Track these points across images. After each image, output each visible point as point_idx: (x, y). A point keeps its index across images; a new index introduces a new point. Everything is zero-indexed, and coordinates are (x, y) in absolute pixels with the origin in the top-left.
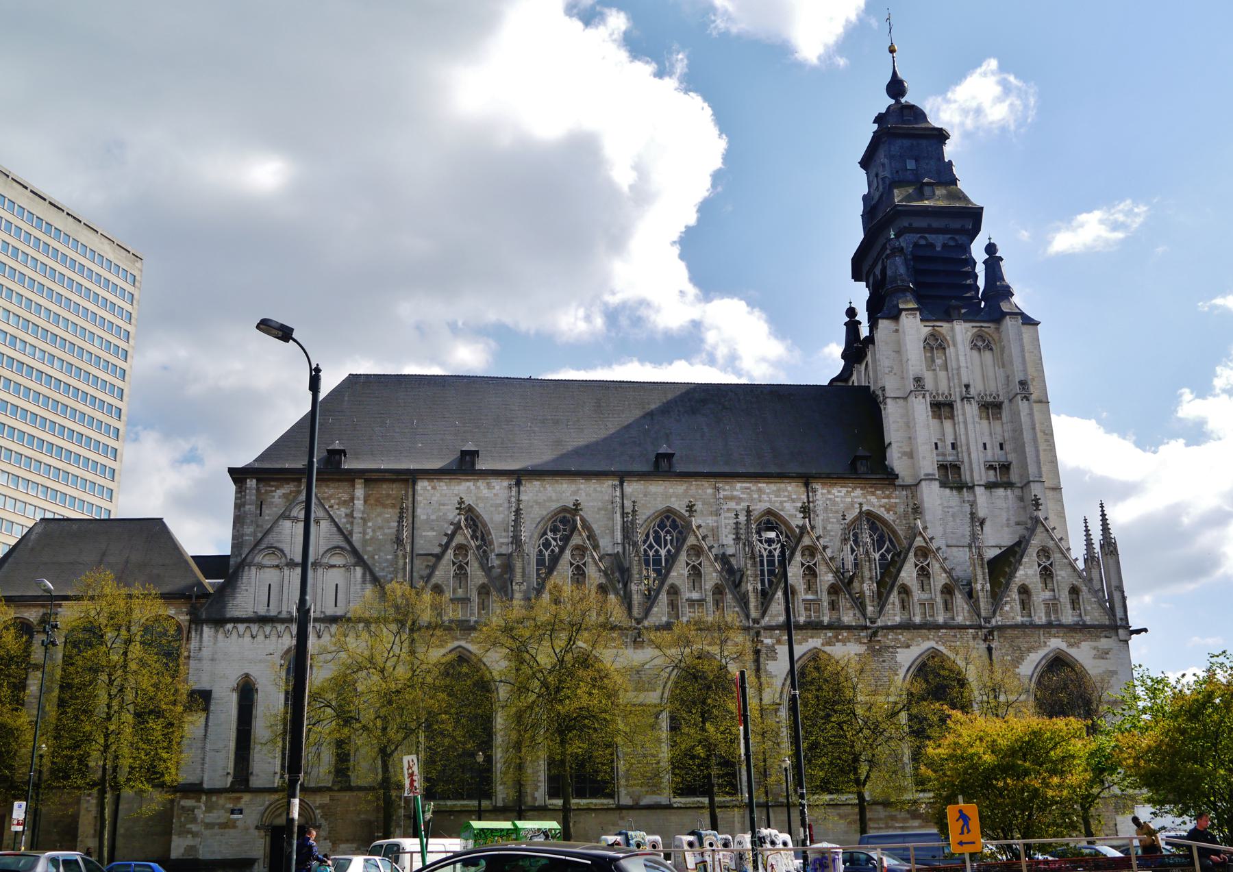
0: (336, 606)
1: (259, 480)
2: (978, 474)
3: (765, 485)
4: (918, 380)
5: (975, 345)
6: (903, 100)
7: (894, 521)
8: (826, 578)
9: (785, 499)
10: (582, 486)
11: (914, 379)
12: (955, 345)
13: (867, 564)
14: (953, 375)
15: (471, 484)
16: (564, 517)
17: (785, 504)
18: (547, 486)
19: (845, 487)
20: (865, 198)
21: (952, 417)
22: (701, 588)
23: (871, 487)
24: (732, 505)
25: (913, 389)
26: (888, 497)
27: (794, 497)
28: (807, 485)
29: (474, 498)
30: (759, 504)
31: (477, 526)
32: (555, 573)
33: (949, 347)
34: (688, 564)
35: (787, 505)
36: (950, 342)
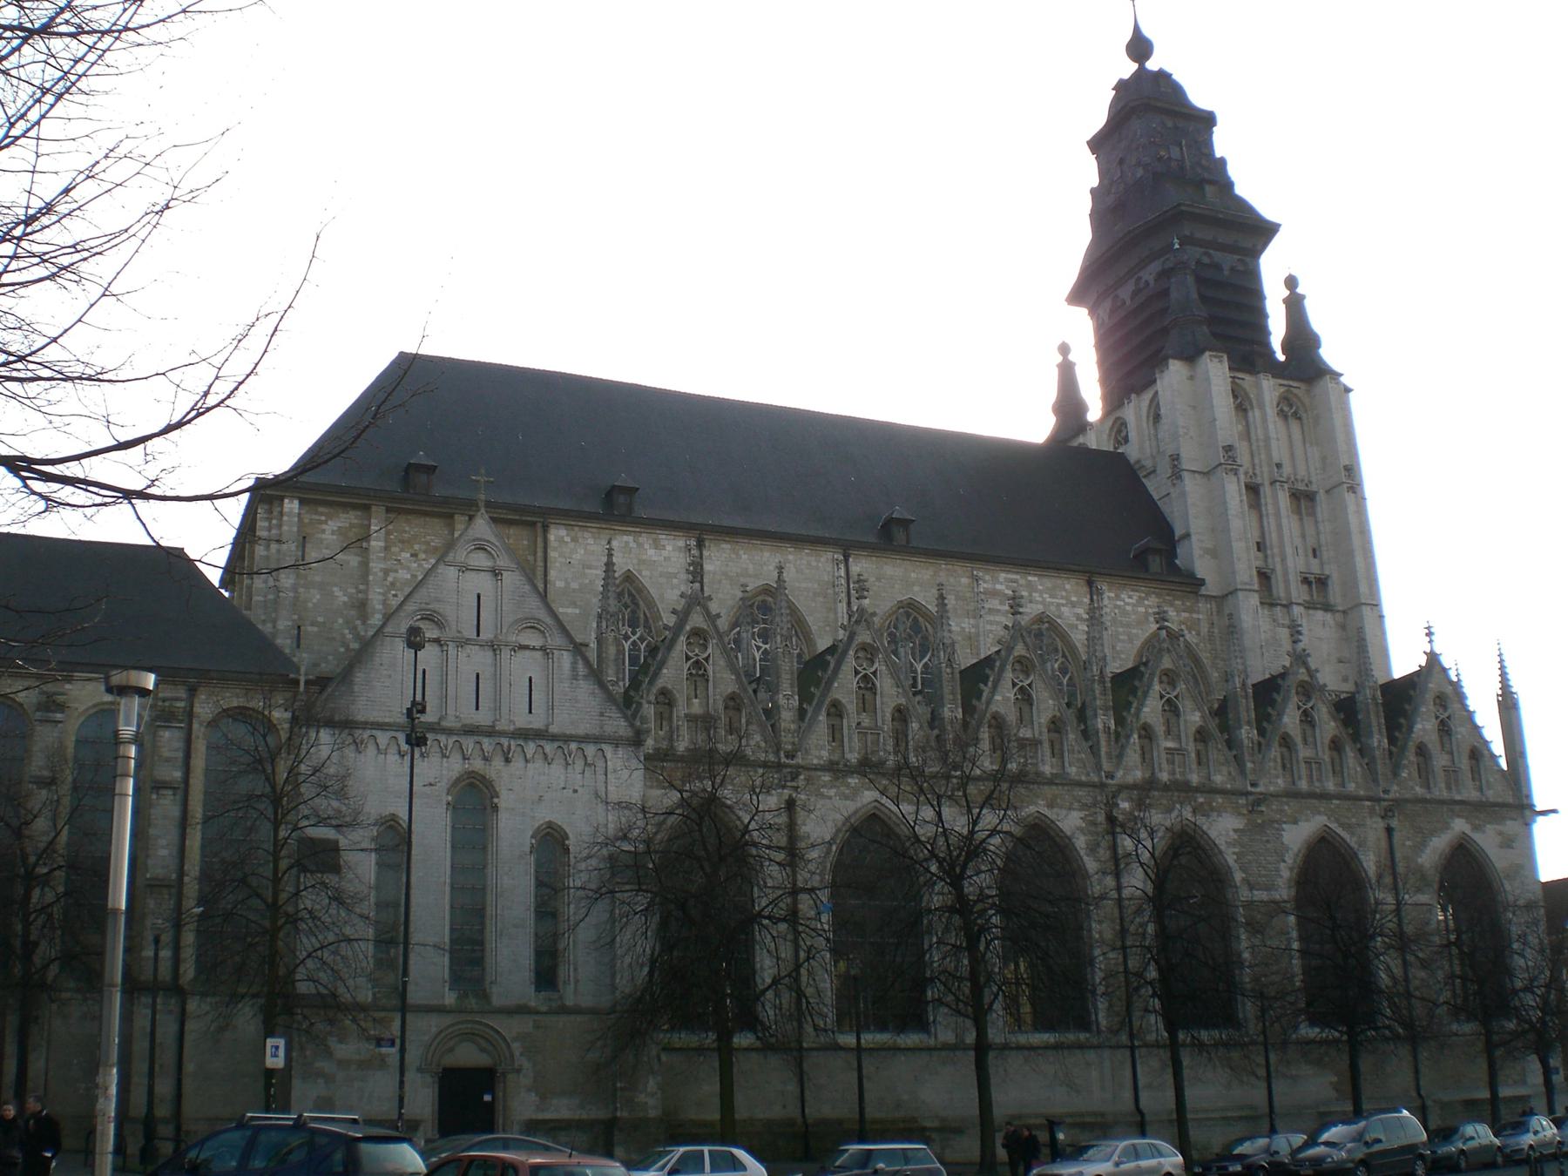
0: (530, 712)
1: (302, 502)
3: (1036, 579)
4: (1229, 449)
5: (1282, 410)
6: (1152, 65)
7: (1197, 645)
8: (1193, 718)
9: (1064, 602)
10: (791, 557)
11: (1223, 447)
12: (1262, 407)
13: (1244, 701)
14: (1258, 446)
15: (630, 538)
16: (764, 601)
17: (1062, 609)
18: (741, 552)
19: (1137, 591)
20: (1093, 191)
22: (1032, 723)
23: (1168, 595)
25: (1223, 461)
26: (1190, 610)
27: (1074, 599)
28: (1090, 583)
29: (635, 561)
30: (1029, 605)
31: (637, 605)
32: (836, 685)
33: (1252, 408)
34: (1014, 685)
36: (1254, 402)
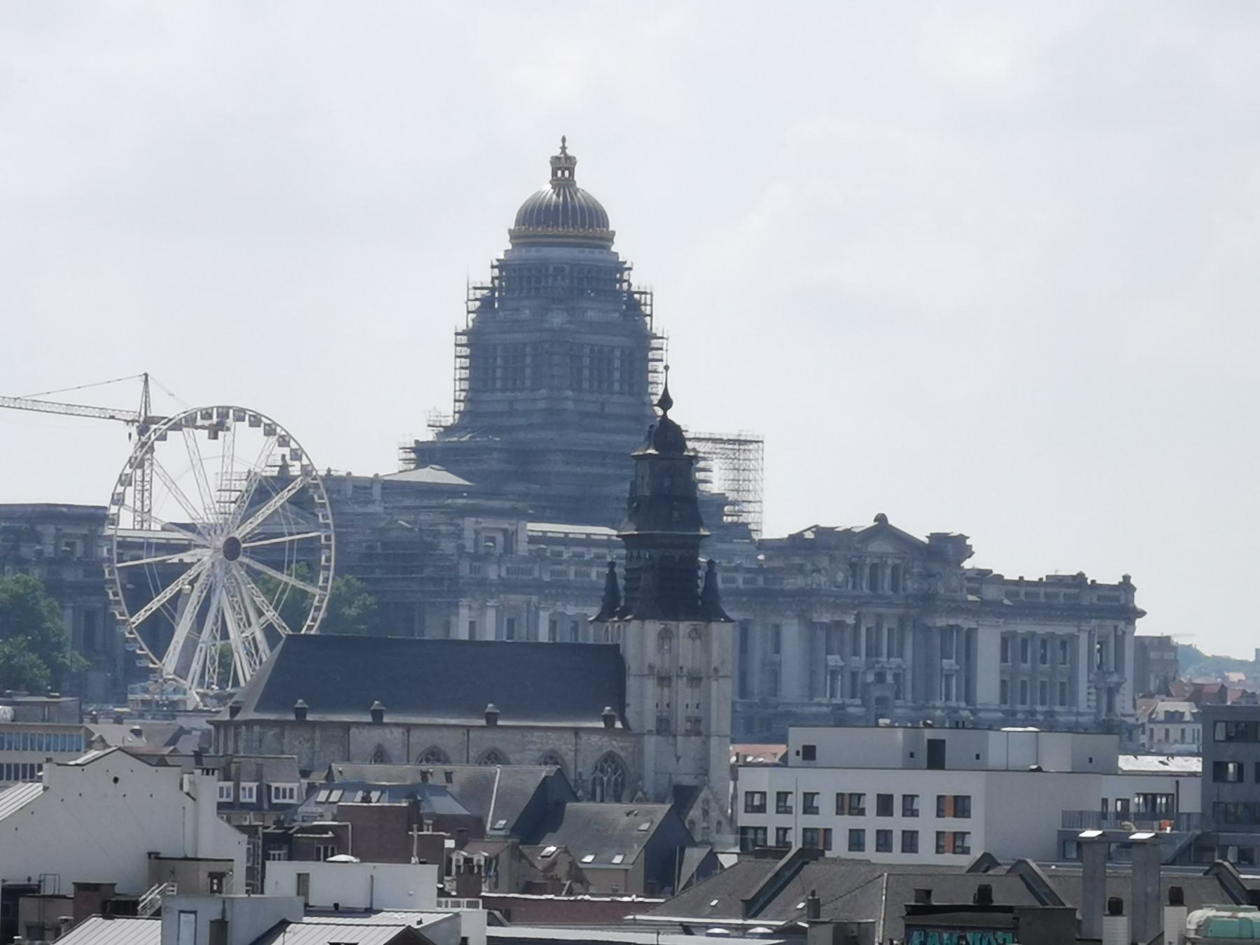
2: (682, 726)
21: (670, 686)
24: (531, 746)
26: (624, 742)
35: (564, 747)
